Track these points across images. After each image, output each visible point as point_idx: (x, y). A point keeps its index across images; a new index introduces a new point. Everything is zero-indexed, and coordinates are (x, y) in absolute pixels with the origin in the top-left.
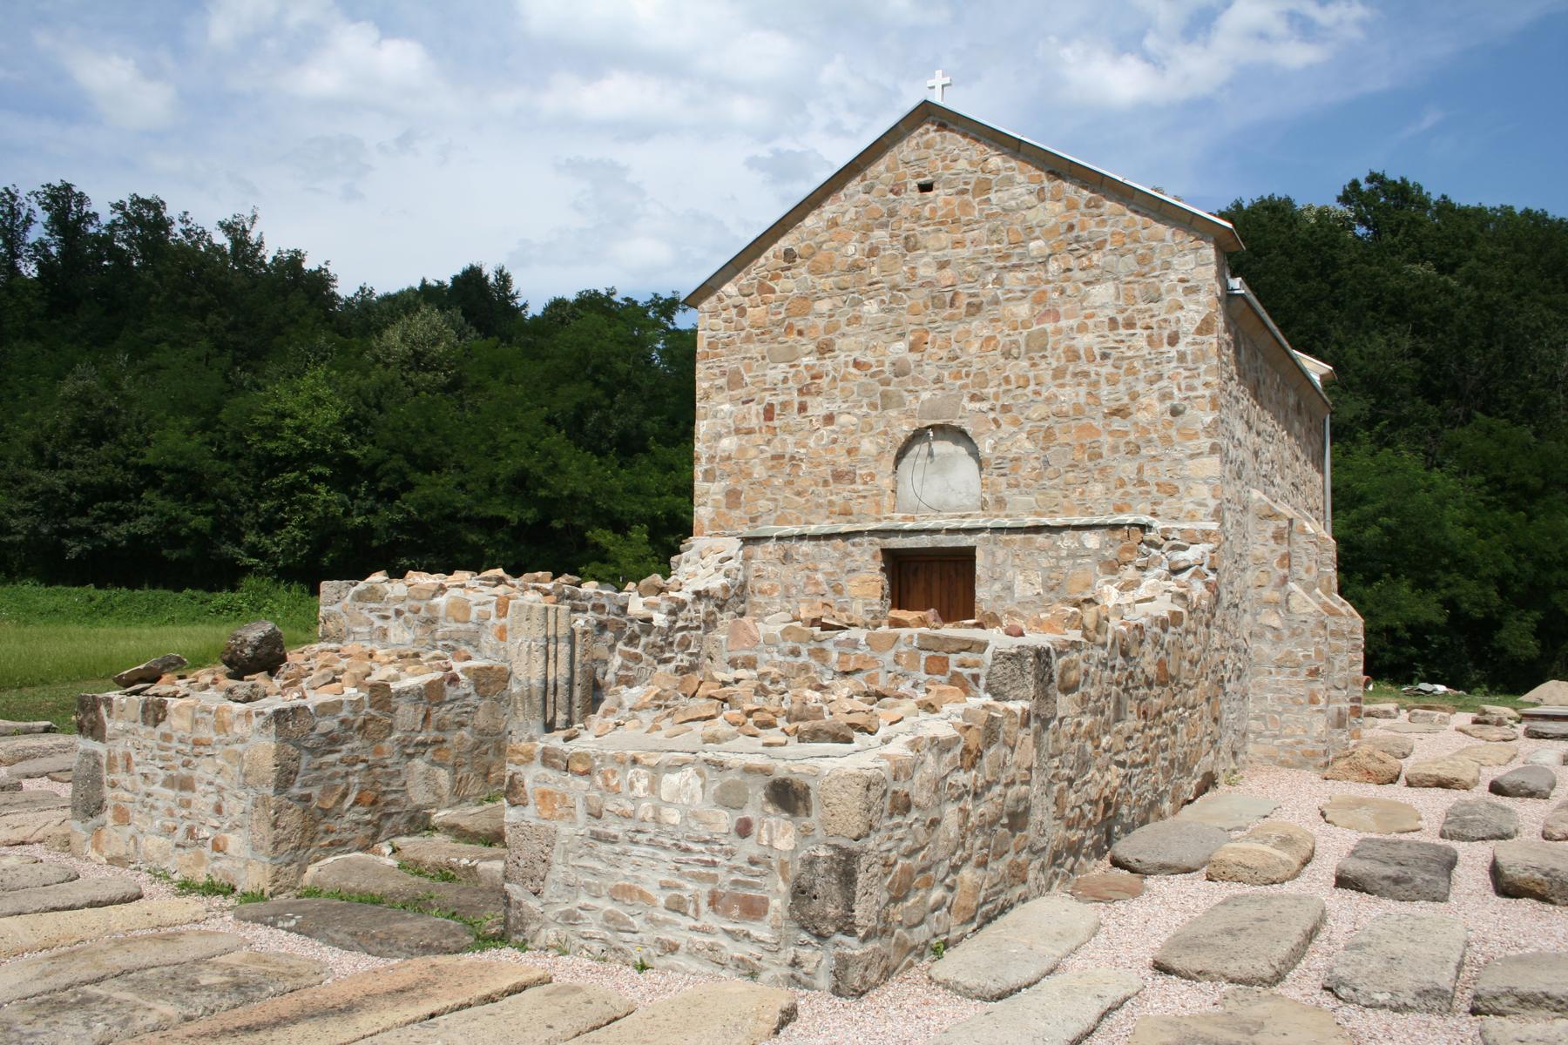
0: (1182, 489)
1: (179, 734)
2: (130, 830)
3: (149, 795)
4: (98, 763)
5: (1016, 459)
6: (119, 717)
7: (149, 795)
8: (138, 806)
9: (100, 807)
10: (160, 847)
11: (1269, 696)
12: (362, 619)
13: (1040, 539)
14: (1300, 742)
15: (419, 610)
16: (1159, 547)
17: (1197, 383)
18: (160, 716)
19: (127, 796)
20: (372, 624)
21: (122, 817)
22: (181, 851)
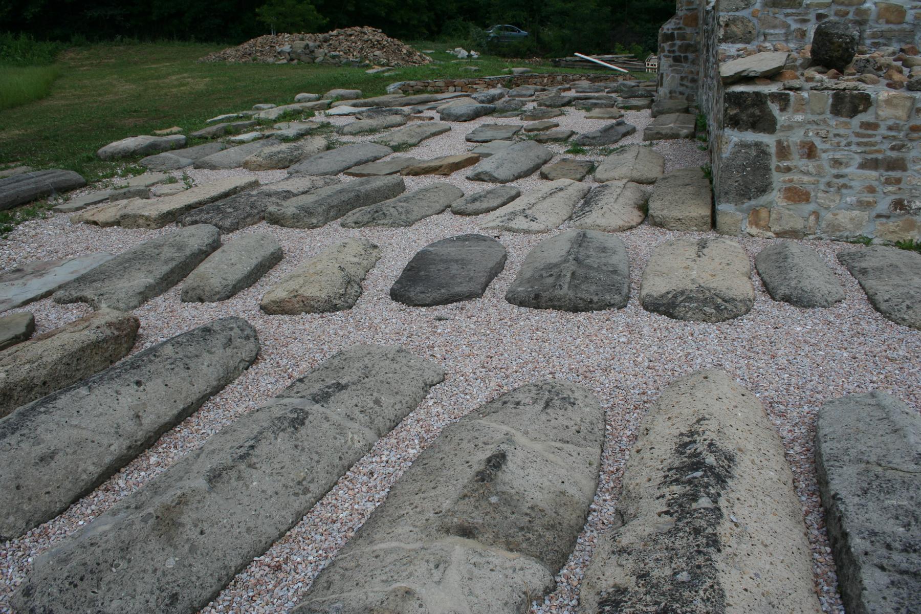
1: (890, 123)
2: (811, 207)
3: (838, 176)
4: (764, 153)
6: (797, 111)
7: (838, 176)
8: (822, 187)
9: (764, 190)
10: (852, 219)
12: (777, 22)
15: (847, 13)
18: (861, 108)
19: (806, 179)
20: (789, 26)
21: (797, 195)
22: (884, 220)
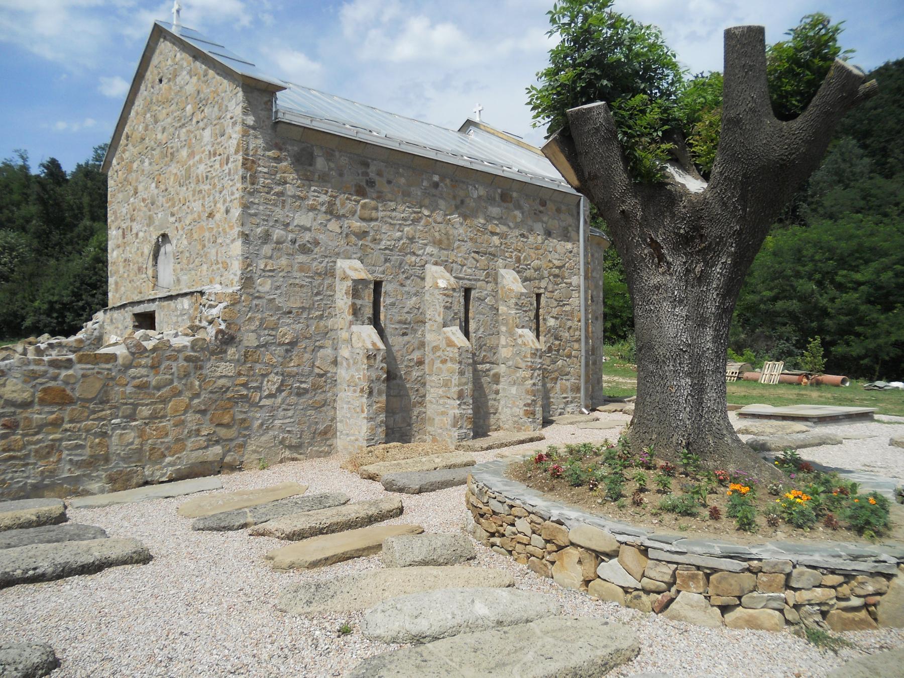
0: (229, 264)
5: (182, 252)
11: (345, 406)
13: (172, 303)
14: (357, 440)
16: (204, 306)
17: (234, 189)
